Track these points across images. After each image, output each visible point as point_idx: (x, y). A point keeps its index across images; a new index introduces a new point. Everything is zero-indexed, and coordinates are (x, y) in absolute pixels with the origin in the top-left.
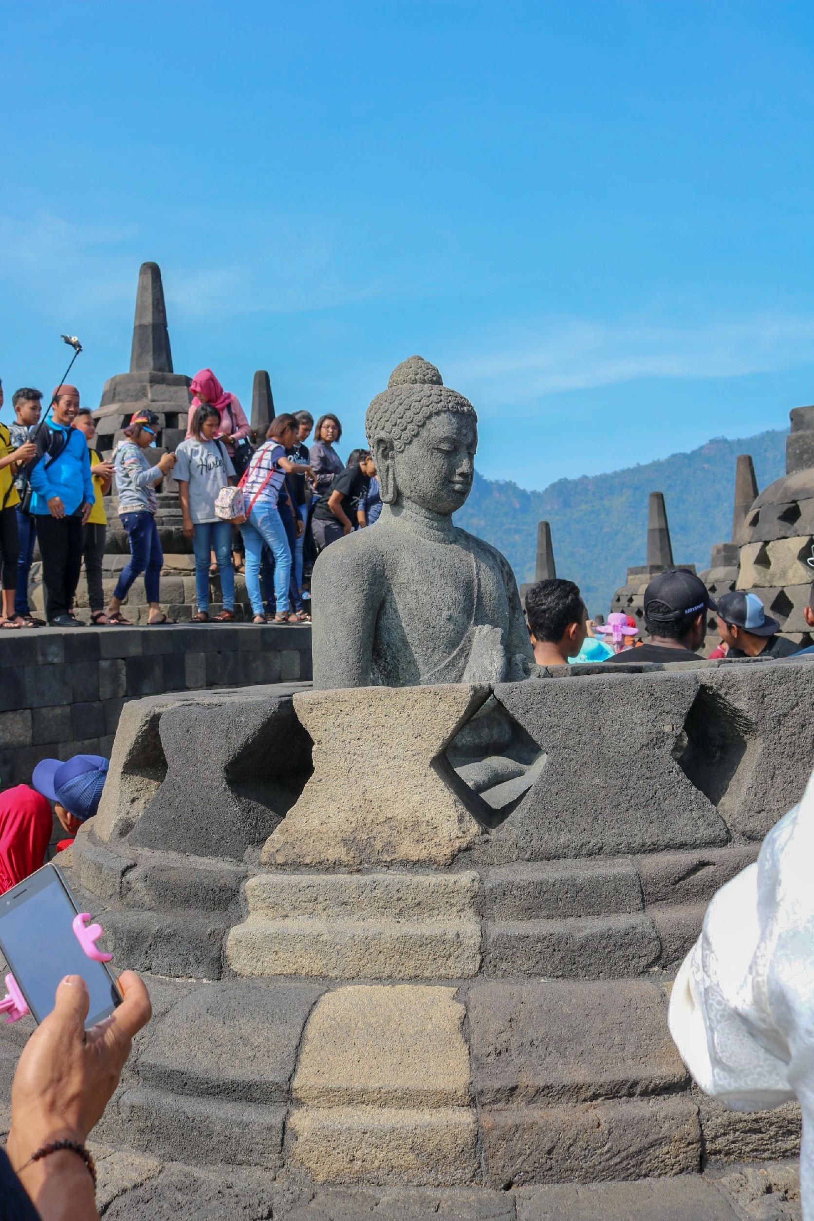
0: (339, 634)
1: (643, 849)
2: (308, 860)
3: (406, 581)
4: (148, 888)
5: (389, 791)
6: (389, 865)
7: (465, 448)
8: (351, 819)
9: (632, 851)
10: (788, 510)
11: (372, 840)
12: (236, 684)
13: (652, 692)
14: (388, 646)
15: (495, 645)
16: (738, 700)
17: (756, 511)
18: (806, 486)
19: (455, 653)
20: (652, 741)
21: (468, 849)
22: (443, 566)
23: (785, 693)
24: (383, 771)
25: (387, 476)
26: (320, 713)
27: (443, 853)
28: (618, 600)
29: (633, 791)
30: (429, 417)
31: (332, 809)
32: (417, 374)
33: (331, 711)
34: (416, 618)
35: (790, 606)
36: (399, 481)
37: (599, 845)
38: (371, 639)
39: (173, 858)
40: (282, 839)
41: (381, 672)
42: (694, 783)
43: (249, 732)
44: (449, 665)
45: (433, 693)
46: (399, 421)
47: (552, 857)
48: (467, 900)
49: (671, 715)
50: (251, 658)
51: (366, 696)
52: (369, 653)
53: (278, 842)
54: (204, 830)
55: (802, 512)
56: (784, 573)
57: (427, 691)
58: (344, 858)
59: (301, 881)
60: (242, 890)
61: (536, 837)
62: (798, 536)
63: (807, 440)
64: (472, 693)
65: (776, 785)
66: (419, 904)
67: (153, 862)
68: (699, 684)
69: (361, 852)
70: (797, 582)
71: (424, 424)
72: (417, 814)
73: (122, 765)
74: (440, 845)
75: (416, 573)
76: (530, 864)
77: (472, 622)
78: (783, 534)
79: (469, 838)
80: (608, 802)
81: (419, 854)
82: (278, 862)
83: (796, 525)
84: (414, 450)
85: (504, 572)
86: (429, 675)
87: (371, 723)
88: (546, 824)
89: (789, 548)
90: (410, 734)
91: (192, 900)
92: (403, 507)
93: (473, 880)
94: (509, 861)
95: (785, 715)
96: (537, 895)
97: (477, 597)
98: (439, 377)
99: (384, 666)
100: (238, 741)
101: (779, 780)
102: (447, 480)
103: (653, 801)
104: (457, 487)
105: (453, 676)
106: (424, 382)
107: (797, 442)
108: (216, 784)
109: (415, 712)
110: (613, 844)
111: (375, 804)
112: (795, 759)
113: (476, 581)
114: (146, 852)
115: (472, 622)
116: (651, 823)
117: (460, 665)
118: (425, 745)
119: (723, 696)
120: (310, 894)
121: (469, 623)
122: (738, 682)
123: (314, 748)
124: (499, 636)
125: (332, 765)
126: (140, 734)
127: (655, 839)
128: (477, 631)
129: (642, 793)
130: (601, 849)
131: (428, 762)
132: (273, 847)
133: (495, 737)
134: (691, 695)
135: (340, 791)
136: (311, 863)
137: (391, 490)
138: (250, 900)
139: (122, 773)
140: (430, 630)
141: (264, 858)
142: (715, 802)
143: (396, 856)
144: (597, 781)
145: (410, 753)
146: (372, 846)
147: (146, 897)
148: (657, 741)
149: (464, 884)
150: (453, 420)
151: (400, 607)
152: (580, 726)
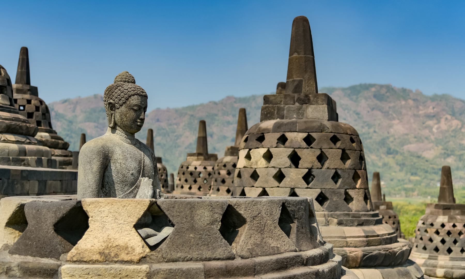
0: (90, 177)
1: (206, 260)
2: (85, 260)
3: (117, 158)
4: (19, 270)
5: (117, 236)
6: (116, 262)
7: (143, 109)
8: (103, 245)
9: (202, 260)
10: (260, 137)
11: (110, 253)
12: (7, 194)
13: (212, 206)
14: (107, 183)
15: (149, 185)
16: (241, 210)
17: (247, 135)
18: (268, 128)
19: (133, 188)
20: (211, 222)
21: (145, 257)
22: (131, 153)
23: (256, 209)
24: (115, 229)
25: (112, 117)
26: (93, 206)
27: (136, 258)
28: (182, 167)
29: (203, 240)
30: (130, 97)
31: (96, 241)
32: (126, 79)
33: (97, 206)
34: (120, 173)
35: (258, 176)
36: (116, 119)
37: (191, 258)
38: (102, 180)
39: (30, 259)
40: (76, 252)
41: (103, 193)
42: (224, 238)
43: (65, 212)
44: (131, 192)
45: (136, 201)
46: (118, 96)
47: (174, 261)
48: (145, 275)
49: (217, 214)
50: (15, 183)
51: (110, 201)
52: (101, 186)
53: (74, 253)
54: (43, 248)
55: (265, 138)
56: (257, 163)
57: (133, 201)
58: (100, 259)
59: (83, 267)
60: (59, 270)
61: (169, 254)
62: (263, 148)
63: (270, 109)
64: (149, 202)
65: (251, 240)
66: (127, 276)
67: (21, 260)
68: (228, 204)
69: (106, 257)
70: (262, 167)
71: (128, 99)
72: (127, 244)
73: (5, 223)
74: (135, 255)
75: (121, 156)
76: (167, 263)
77: (141, 176)
78: (257, 146)
79: (146, 253)
80: (195, 243)
81: (127, 258)
82: (74, 260)
83: (263, 143)
84: (123, 108)
85: (153, 157)
86: (122, 195)
87: (112, 211)
88: (173, 249)
89: (259, 153)
90: (127, 216)
91: (38, 274)
92: (117, 130)
93: (147, 268)
94: (159, 262)
95: (256, 216)
96: (169, 273)
97: (143, 167)
98: (135, 81)
99: (105, 191)
100: (60, 215)
101: (252, 238)
102: (135, 121)
103: (210, 243)
104: (139, 124)
105: (132, 196)
106: (128, 82)
107: (266, 109)
108: (49, 231)
109: (129, 208)
110: (196, 257)
111: (112, 240)
112: (258, 232)
113: (143, 160)
114: (17, 256)
115: (141, 176)
116: (209, 251)
117: (135, 192)
118: (132, 220)
119: (236, 209)
120: (87, 271)
121: (139, 176)
122: (241, 204)
123: (90, 219)
124: (151, 183)
125: (96, 225)
126: (15, 211)
127: (210, 256)
128: (143, 180)
129: (207, 240)
130: (191, 259)
131: (132, 226)
132: (72, 255)
133: (146, 221)
134: (225, 207)
135: (99, 235)
136: (87, 261)
137: (112, 123)
138: (63, 274)
139: (6, 226)
140: (125, 178)
141: (68, 259)
142: (231, 245)
143: (119, 259)
144: (191, 235)
145: (126, 222)
146: (110, 255)
147: (18, 273)
148: (212, 223)
149: (144, 269)
150: (139, 98)
151: (113, 167)
152: (186, 216)
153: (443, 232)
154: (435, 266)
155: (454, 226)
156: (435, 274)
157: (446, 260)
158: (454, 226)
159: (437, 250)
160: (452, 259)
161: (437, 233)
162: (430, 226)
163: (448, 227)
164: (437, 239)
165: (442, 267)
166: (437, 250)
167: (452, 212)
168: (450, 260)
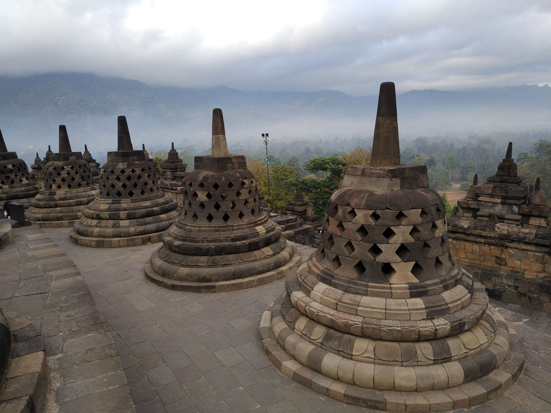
153: (123, 177)
154: (119, 210)
155: (133, 171)
156: (119, 216)
157: (129, 202)
158: (133, 171)
159: (119, 194)
160: (134, 201)
161: (118, 179)
162: (111, 174)
163: (128, 172)
164: (119, 185)
165: (125, 210)
166: (119, 194)
167: (131, 158)
168: (132, 202)
